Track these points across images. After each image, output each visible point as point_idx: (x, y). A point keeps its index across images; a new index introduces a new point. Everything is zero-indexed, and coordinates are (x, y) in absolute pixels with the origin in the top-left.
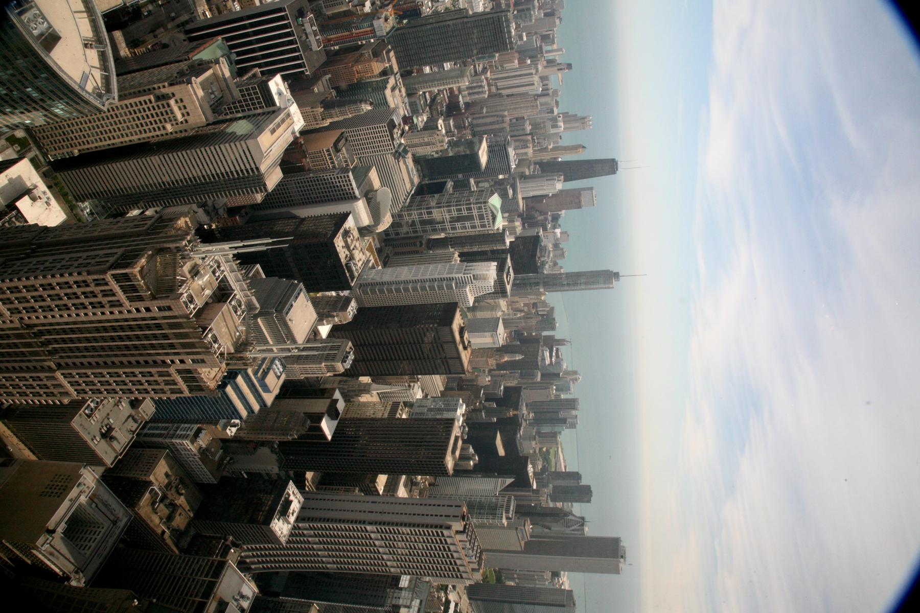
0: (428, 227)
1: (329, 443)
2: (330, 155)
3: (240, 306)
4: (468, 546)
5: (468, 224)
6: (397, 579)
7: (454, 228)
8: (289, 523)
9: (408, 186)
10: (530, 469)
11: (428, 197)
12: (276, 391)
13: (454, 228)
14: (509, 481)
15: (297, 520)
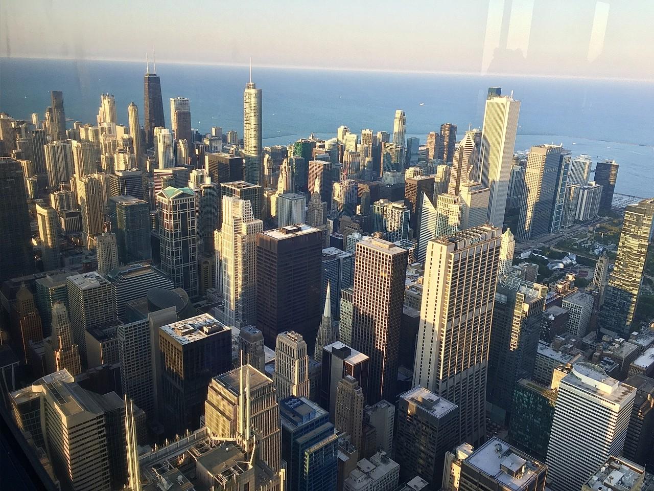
0: (191, 255)
1: (370, 358)
2: (108, 345)
3: (202, 445)
4: (470, 240)
5: (189, 219)
6: (498, 305)
7: (193, 232)
8: (438, 401)
9: (149, 271)
10: (418, 178)
11: (162, 254)
12: (315, 407)
13: (193, 232)
14: (426, 198)
15: (437, 393)
